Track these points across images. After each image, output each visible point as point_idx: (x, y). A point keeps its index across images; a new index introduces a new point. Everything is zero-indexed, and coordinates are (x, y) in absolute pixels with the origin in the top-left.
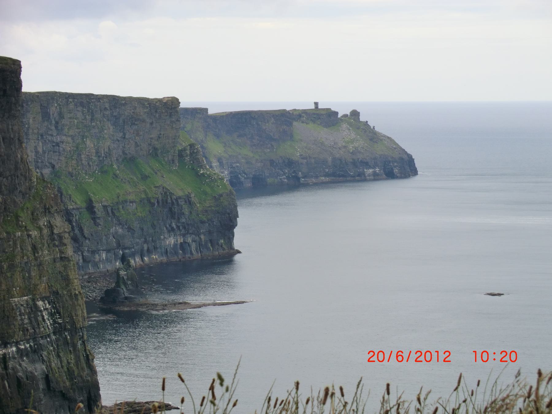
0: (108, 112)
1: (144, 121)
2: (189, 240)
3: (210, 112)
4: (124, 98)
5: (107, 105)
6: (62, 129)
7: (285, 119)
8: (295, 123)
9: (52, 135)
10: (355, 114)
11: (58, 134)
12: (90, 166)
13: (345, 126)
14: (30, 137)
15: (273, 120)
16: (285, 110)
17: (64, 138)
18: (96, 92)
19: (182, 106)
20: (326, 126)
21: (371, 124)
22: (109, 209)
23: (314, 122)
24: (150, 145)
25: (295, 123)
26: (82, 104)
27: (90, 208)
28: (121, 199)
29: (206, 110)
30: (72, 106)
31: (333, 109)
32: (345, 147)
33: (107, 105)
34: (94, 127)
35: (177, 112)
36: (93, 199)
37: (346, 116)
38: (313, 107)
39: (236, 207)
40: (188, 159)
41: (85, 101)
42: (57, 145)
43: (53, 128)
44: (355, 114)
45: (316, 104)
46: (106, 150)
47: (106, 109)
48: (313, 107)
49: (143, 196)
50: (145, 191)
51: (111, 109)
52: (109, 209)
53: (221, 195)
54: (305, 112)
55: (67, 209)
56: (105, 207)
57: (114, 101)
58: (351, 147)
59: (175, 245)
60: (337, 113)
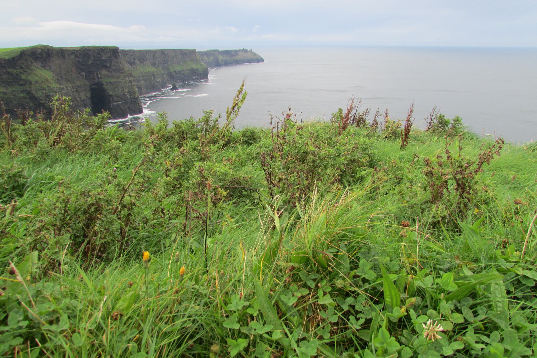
3: (220, 50)
7: (236, 51)
10: (251, 50)
27: (175, 72)
44: (251, 50)
57: (181, 50)
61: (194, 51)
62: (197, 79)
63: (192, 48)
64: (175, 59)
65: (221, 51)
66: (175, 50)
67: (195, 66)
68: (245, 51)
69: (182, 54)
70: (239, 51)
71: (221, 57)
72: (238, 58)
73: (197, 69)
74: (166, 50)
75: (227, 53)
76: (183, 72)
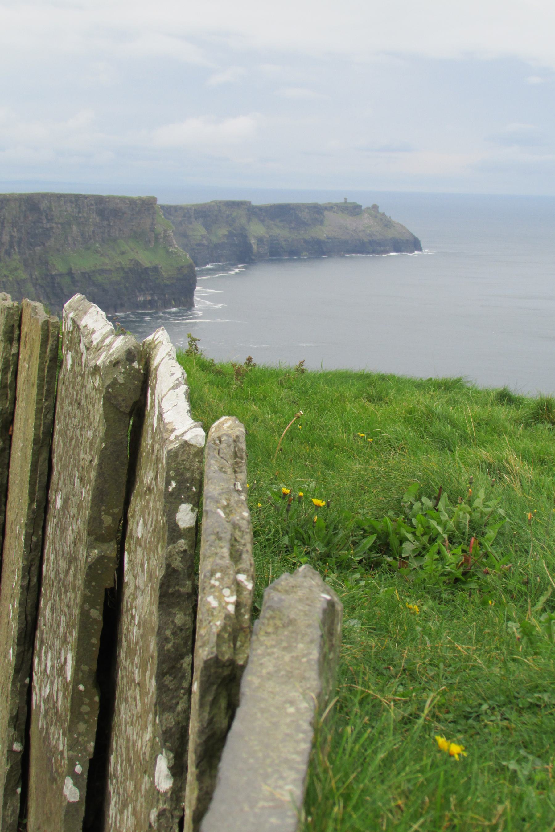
0: (94, 207)
1: (124, 213)
2: (156, 298)
4: (108, 197)
5: (93, 202)
6: (52, 219)
8: (326, 213)
9: (42, 223)
10: (375, 207)
11: (48, 222)
12: (75, 244)
13: (366, 215)
14: (5, 225)
15: (307, 210)
16: (316, 204)
17: (54, 225)
18: (83, 193)
19: (160, 202)
20: (351, 215)
21: (388, 214)
22: (87, 275)
23: (343, 212)
24: (131, 230)
25: (326, 213)
26: (71, 202)
27: (70, 273)
28: (98, 268)
29: (250, 203)
30: (62, 203)
31: (359, 203)
32: (364, 231)
33: (93, 202)
34: (80, 217)
35: (153, 207)
36: (73, 268)
37: (368, 208)
38: (343, 201)
39: (195, 276)
40: (161, 240)
41: (73, 199)
42: (47, 229)
43: (44, 217)
44: (375, 207)
45: (346, 199)
46: (91, 233)
47: (92, 205)
48: (343, 201)
49: (118, 266)
50: (120, 263)
51: (96, 204)
52: (87, 275)
53: (182, 267)
54: (337, 205)
55: (51, 275)
56: (84, 274)
57: (100, 200)
58: (368, 231)
59: (144, 301)
60: (360, 207)
61: (147, 206)
62: (151, 304)
63: (144, 195)
64: (74, 228)
65: (261, 209)
66: (77, 200)
67: (145, 258)
68: (354, 210)
69: (101, 213)
70: (330, 208)
71: (257, 230)
72: (322, 232)
73: (155, 269)
74: (44, 196)
75: (282, 213)
76: (99, 279)
